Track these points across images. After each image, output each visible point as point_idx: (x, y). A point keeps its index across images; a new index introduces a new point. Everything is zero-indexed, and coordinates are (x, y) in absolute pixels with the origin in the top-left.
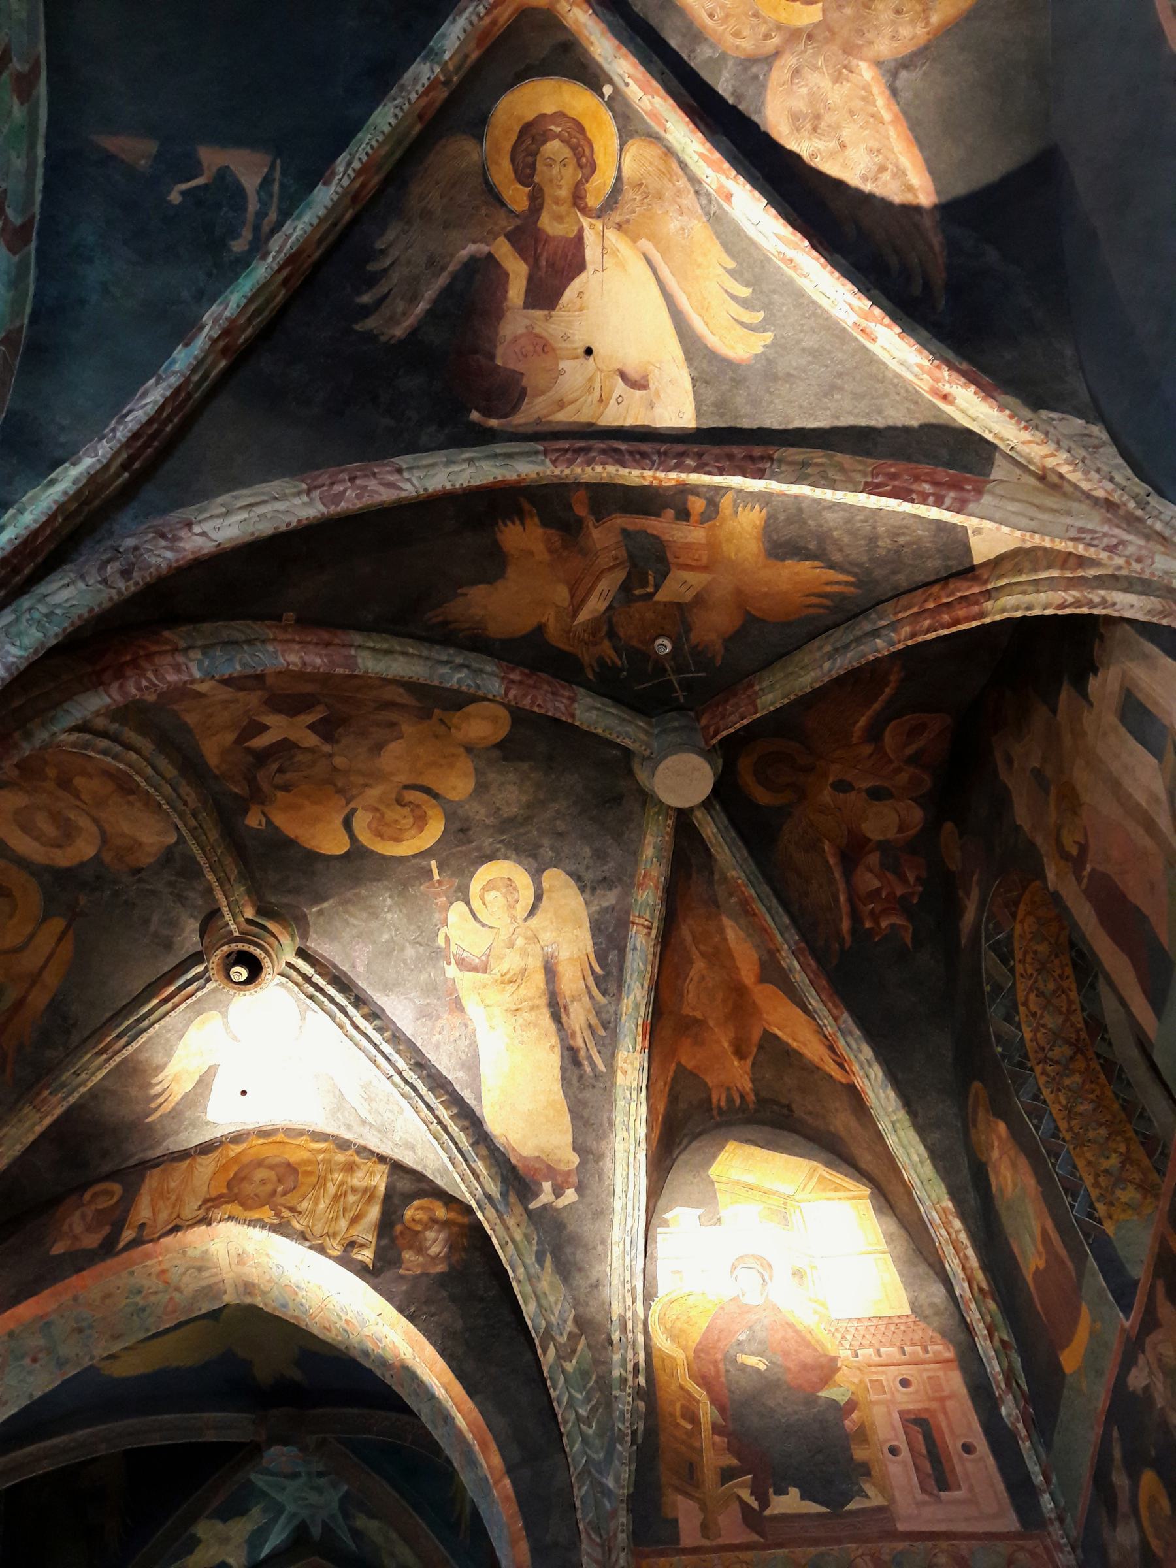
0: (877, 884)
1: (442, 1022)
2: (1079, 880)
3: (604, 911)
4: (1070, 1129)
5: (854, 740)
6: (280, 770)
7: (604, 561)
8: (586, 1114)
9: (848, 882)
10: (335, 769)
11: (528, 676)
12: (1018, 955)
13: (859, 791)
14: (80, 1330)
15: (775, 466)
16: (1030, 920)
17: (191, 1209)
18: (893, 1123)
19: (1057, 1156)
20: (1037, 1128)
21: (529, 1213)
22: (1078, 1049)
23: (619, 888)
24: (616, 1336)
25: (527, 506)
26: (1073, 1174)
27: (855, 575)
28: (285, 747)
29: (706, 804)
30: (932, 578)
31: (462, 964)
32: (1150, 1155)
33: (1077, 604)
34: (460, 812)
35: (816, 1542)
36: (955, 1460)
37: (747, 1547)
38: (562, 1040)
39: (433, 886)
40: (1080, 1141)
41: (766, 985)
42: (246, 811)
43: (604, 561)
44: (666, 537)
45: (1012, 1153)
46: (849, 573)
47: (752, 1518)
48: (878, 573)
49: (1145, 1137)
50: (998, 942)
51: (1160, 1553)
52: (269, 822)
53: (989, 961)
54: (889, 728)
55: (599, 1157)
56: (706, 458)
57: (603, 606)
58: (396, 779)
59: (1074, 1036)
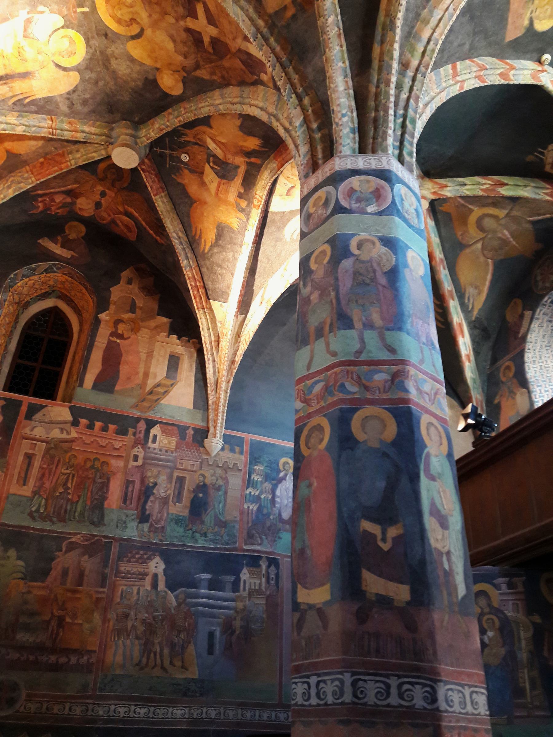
0: (58, 201)
3: (57, 105)
5: (126, 207)
7: (229, 156)
12: (48, 275)
16: (64, 280)
23: (69, 112)
28: (193, 15)
30: (205, 282)
34: (119, 41)
39: (74, 7)
41: (6, 153)
43: (229, 156)
44: (232, 185)
46: (209, 251)
48: (208, 263)
50: (53, 268)
53: (44, 265)
59: (22, 299)
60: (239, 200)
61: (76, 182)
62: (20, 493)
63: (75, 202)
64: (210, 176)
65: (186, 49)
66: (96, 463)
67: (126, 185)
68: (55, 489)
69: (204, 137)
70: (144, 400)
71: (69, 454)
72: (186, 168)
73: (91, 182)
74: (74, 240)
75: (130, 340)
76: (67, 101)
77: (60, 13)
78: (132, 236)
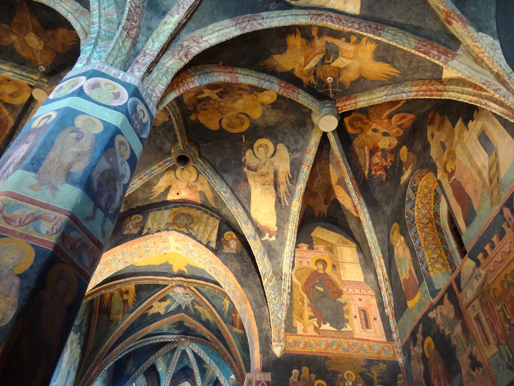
1: (241, 184)
2: (449, 180)
4: (424, 244)
5: (383, 118)
6: (204, 105)
8: (281, 216)
9: (370, 160)
10: (220, 106)
11: (286, 85)
12: (419, 191)
13: (380, 132)
14: (131, 255)
15: (385, 33)
16: (425, 182)
17: (163, 226)
18: (370, 231)
19: (419, 251)
20: (415, 242)
21: (262, 241)
22: (430, 221)
24: (283, 278)
25: (298, 31)
26: (423, 257)
27: (401, 71)
28: (208, 98)
29: (333, 132)
31: (249, 168)
32: (446, 256)
33: (476, 102)
35: (333, 337)
36: (371, 321)
37: (315, 336)
38: (277, 195)
40: (427, 248)
42: (191, 114)
43: (318, 51)
45: (404, 246)
46: (399, 70)
47: (316, 329)
49: (446, 250)
51: (428, 357)
52: (197, 119)
53: (409, 191)
54: (395, 115)
55: (283, 229)
56: (362, 25)
57: (314, 65)
58: (238, 111)
60: (352, 42)
61: (363, 147)
62: (492, 353)
63: (382, 149)
64: (340, 62)
65: (235, 96)
66: (508, 280)
67: (364, 116)
68: (504, 329)
69: (305, 71)
70: (492, 192)
71: (491, 291)
72: (339, 79)
73: (364, 138)
74: (407, 159)
75: (457, 168)
76: (294, 153)
77: (246, 151)
78: (410, 117)
